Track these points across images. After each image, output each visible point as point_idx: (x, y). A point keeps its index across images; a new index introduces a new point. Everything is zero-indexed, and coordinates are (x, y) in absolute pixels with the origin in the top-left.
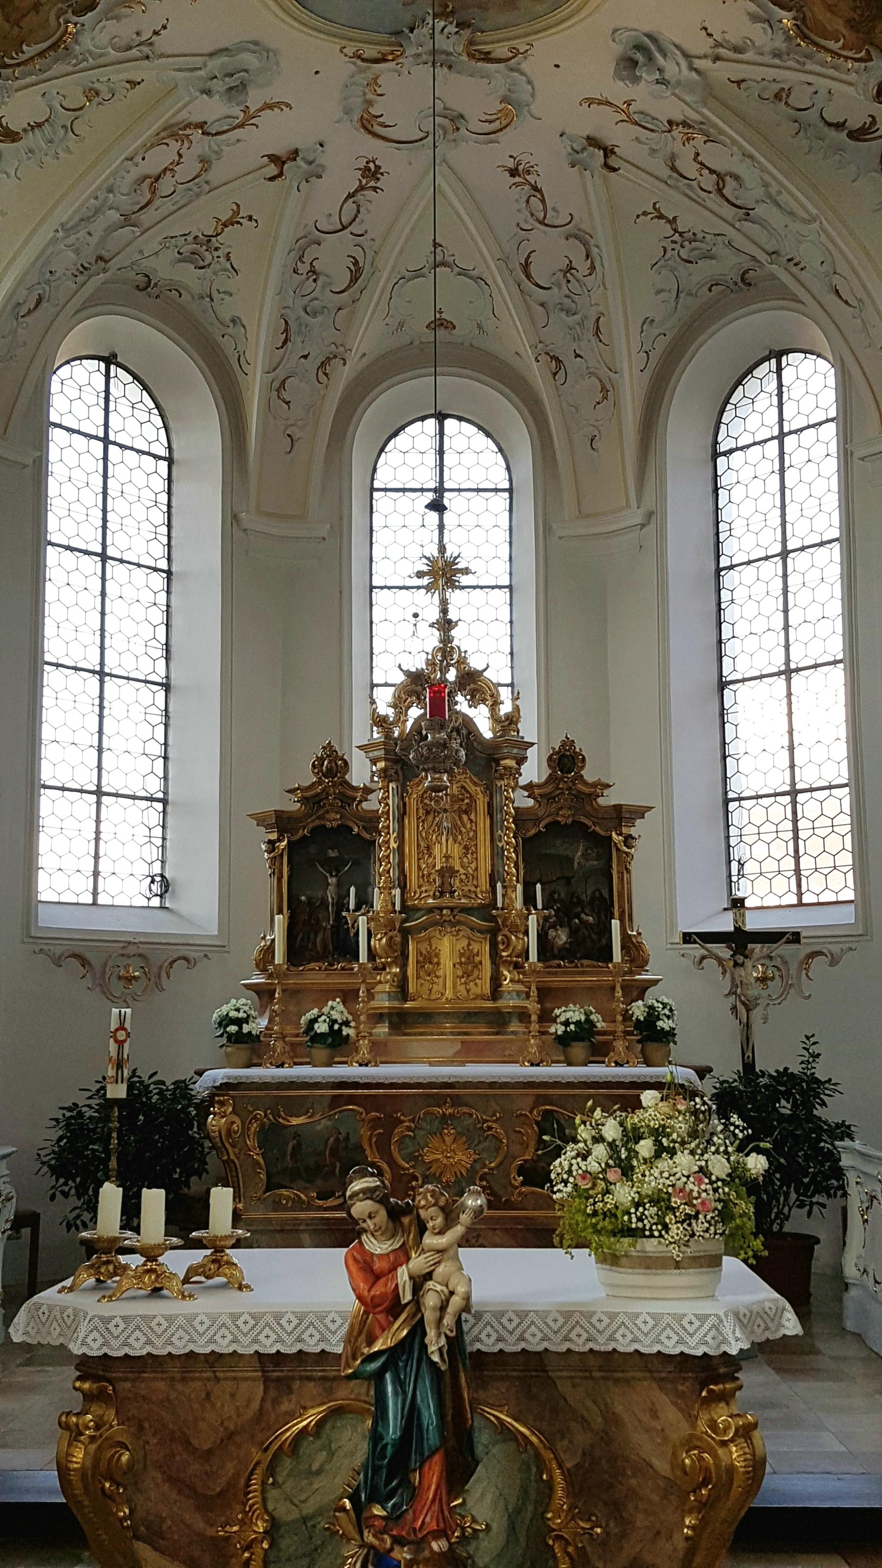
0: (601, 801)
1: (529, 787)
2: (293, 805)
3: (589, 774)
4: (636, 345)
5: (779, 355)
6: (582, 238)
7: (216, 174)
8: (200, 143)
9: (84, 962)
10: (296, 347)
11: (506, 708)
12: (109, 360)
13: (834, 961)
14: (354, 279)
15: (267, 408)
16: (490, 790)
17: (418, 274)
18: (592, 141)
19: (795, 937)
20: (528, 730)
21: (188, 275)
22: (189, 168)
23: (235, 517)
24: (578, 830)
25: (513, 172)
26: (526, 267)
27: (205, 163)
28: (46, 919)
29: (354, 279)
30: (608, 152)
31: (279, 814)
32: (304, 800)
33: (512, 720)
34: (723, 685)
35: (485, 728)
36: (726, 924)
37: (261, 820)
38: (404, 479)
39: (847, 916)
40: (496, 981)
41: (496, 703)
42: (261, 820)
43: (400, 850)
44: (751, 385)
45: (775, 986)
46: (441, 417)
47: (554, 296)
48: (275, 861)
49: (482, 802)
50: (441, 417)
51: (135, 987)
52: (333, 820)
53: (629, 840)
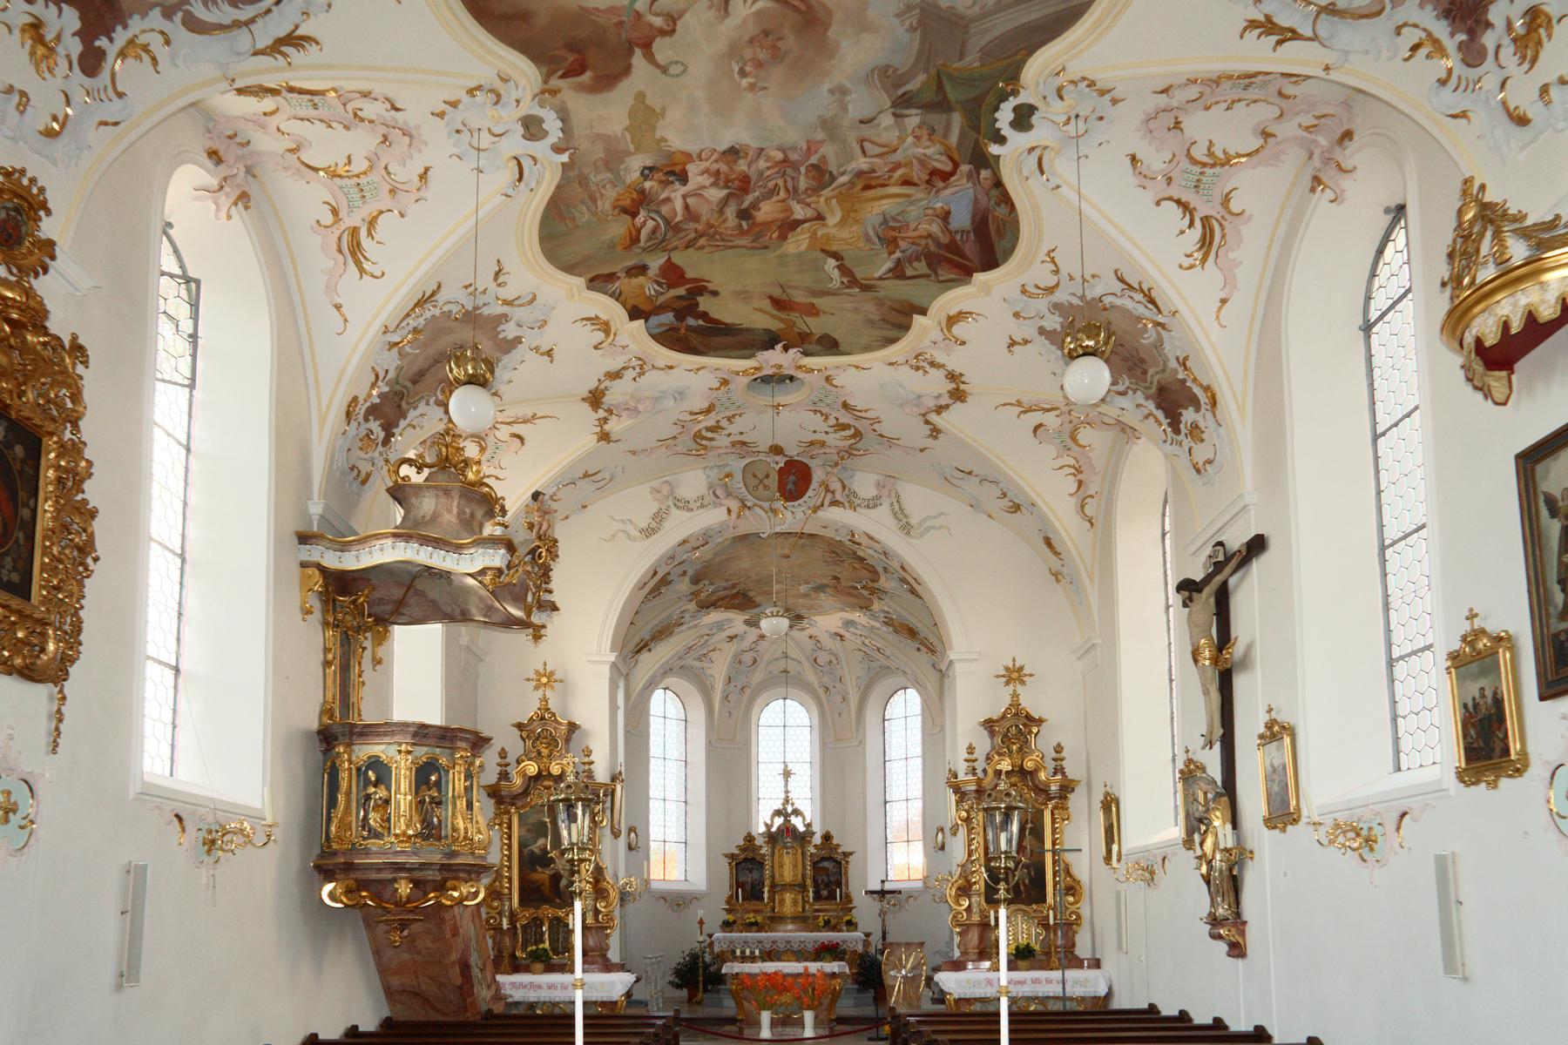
0: (839, 851)
1: (815, 846)
2: (736, 851)
3: (835, 842)
4: (854, 684)
5: (905, 688)
6: (835, 655)
7: (709, 643)
8: (706, 637)
9: (665, 899)
10: (733, 684)
11: (808, 821)
12: (665, 689)
13: (915, 899)
14: (754, 663)
15: (722, 704)
16: (803, 848)
17: (777, 659)
18: (837, 634)
19: (900, 892)
20: (817, 828)
21: (697, 664)
22: (702, 641)
23: (710, 742)
24: (831, 859)
25: (811, 637)
26: (815, 660)
27: (706, 641)
28: (654, 886)
29: (754, 663)
30: (841, 636)
31: (732, 854)
32: (740, 850)
33: (808, 825)
34: (886, 803)
35: (802, 829)
36: (878, 888)
37: (726, 856)
38: (770, 722)
39: (920, 884)
40: (804, 907)
41: (804, 819)
42: (726, 856)
43: (772, 867)
44: (896, 697)
45: (898, 907)
46: (785, 699)
47: (825, 669)
48: (731, 869)
49: (799, 852)
50: (785, 699)
51: (682, 907)
52: (750, 855)
53: (847, 862)
